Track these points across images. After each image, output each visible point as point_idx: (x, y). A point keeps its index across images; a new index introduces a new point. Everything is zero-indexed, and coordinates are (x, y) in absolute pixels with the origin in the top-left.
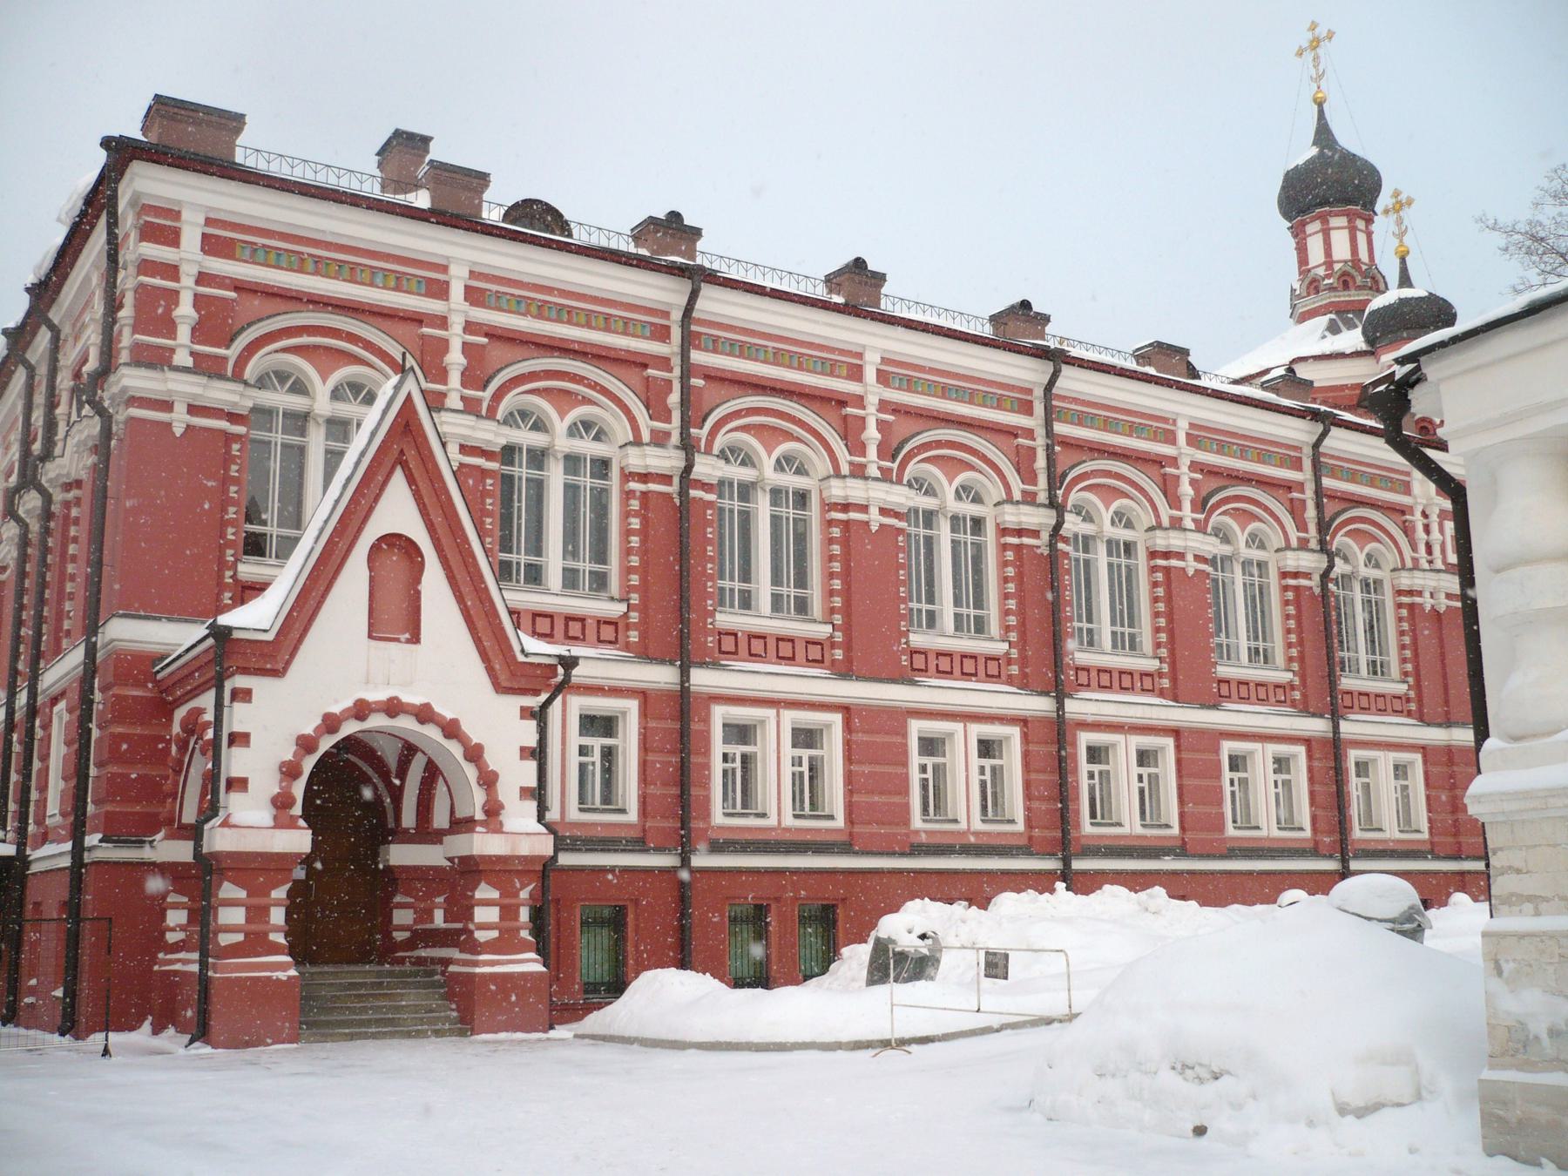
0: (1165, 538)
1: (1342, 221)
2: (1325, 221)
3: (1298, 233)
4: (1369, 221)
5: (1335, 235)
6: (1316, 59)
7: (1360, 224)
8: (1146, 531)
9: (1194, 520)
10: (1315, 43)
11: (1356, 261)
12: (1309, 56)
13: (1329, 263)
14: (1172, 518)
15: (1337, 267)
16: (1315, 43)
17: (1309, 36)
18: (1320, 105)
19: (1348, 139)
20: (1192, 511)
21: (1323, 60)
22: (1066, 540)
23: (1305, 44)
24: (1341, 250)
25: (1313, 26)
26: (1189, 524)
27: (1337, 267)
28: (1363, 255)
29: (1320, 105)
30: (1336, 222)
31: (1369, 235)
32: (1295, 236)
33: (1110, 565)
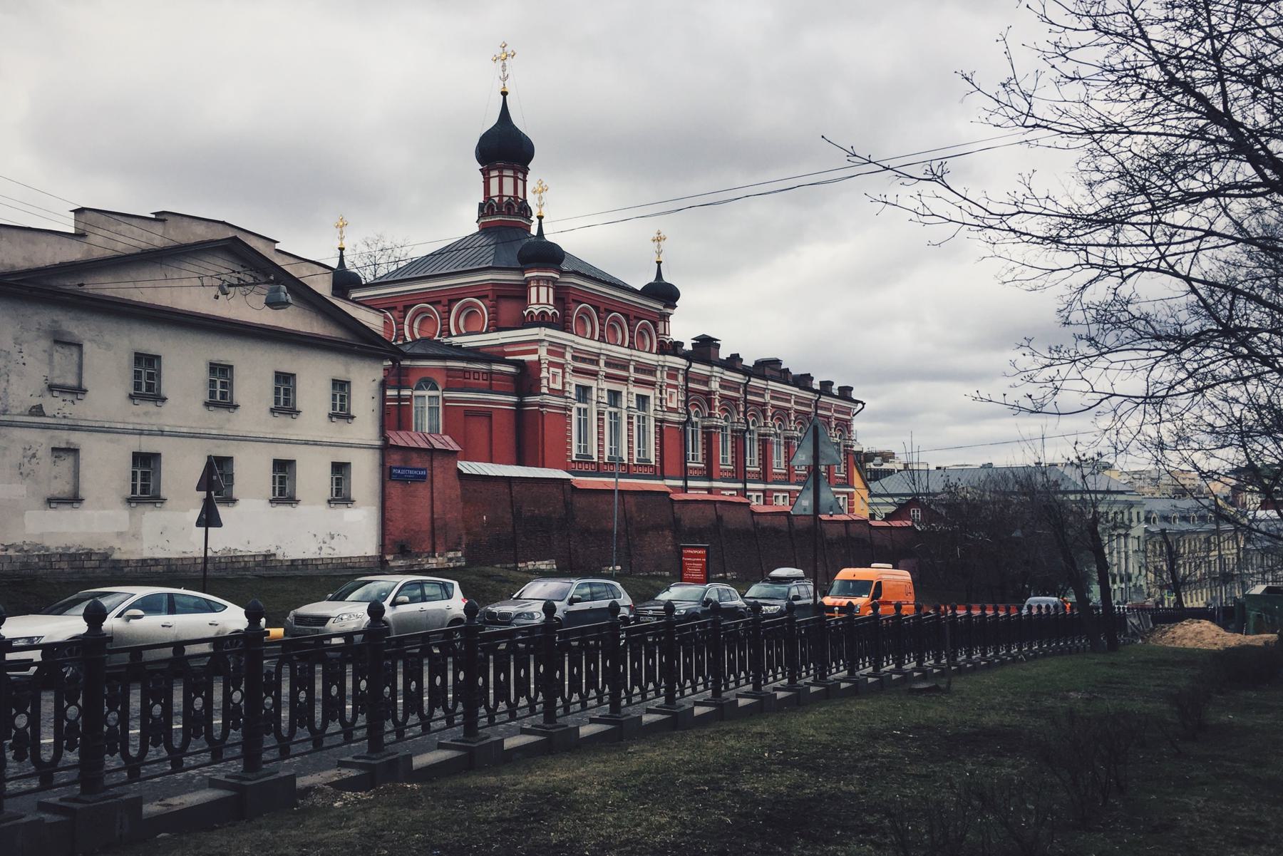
1: (510, 173)
2: (501, 172)
3: (486, 173)
4: (525, 174)
5: (505, 180)
6: (504, 66)
7: (520, 176)
11: (516, 197)
13: (501, 196)
15: (505, 199)
18: (504, 94)
19: (519, 120)
21: (507, 68)
24: (508, 190)
27: (505, 199)
28: (520, 195)
29: (504, 94)
30: (506, 173)
31: (525, 181)
32: (484, 175)
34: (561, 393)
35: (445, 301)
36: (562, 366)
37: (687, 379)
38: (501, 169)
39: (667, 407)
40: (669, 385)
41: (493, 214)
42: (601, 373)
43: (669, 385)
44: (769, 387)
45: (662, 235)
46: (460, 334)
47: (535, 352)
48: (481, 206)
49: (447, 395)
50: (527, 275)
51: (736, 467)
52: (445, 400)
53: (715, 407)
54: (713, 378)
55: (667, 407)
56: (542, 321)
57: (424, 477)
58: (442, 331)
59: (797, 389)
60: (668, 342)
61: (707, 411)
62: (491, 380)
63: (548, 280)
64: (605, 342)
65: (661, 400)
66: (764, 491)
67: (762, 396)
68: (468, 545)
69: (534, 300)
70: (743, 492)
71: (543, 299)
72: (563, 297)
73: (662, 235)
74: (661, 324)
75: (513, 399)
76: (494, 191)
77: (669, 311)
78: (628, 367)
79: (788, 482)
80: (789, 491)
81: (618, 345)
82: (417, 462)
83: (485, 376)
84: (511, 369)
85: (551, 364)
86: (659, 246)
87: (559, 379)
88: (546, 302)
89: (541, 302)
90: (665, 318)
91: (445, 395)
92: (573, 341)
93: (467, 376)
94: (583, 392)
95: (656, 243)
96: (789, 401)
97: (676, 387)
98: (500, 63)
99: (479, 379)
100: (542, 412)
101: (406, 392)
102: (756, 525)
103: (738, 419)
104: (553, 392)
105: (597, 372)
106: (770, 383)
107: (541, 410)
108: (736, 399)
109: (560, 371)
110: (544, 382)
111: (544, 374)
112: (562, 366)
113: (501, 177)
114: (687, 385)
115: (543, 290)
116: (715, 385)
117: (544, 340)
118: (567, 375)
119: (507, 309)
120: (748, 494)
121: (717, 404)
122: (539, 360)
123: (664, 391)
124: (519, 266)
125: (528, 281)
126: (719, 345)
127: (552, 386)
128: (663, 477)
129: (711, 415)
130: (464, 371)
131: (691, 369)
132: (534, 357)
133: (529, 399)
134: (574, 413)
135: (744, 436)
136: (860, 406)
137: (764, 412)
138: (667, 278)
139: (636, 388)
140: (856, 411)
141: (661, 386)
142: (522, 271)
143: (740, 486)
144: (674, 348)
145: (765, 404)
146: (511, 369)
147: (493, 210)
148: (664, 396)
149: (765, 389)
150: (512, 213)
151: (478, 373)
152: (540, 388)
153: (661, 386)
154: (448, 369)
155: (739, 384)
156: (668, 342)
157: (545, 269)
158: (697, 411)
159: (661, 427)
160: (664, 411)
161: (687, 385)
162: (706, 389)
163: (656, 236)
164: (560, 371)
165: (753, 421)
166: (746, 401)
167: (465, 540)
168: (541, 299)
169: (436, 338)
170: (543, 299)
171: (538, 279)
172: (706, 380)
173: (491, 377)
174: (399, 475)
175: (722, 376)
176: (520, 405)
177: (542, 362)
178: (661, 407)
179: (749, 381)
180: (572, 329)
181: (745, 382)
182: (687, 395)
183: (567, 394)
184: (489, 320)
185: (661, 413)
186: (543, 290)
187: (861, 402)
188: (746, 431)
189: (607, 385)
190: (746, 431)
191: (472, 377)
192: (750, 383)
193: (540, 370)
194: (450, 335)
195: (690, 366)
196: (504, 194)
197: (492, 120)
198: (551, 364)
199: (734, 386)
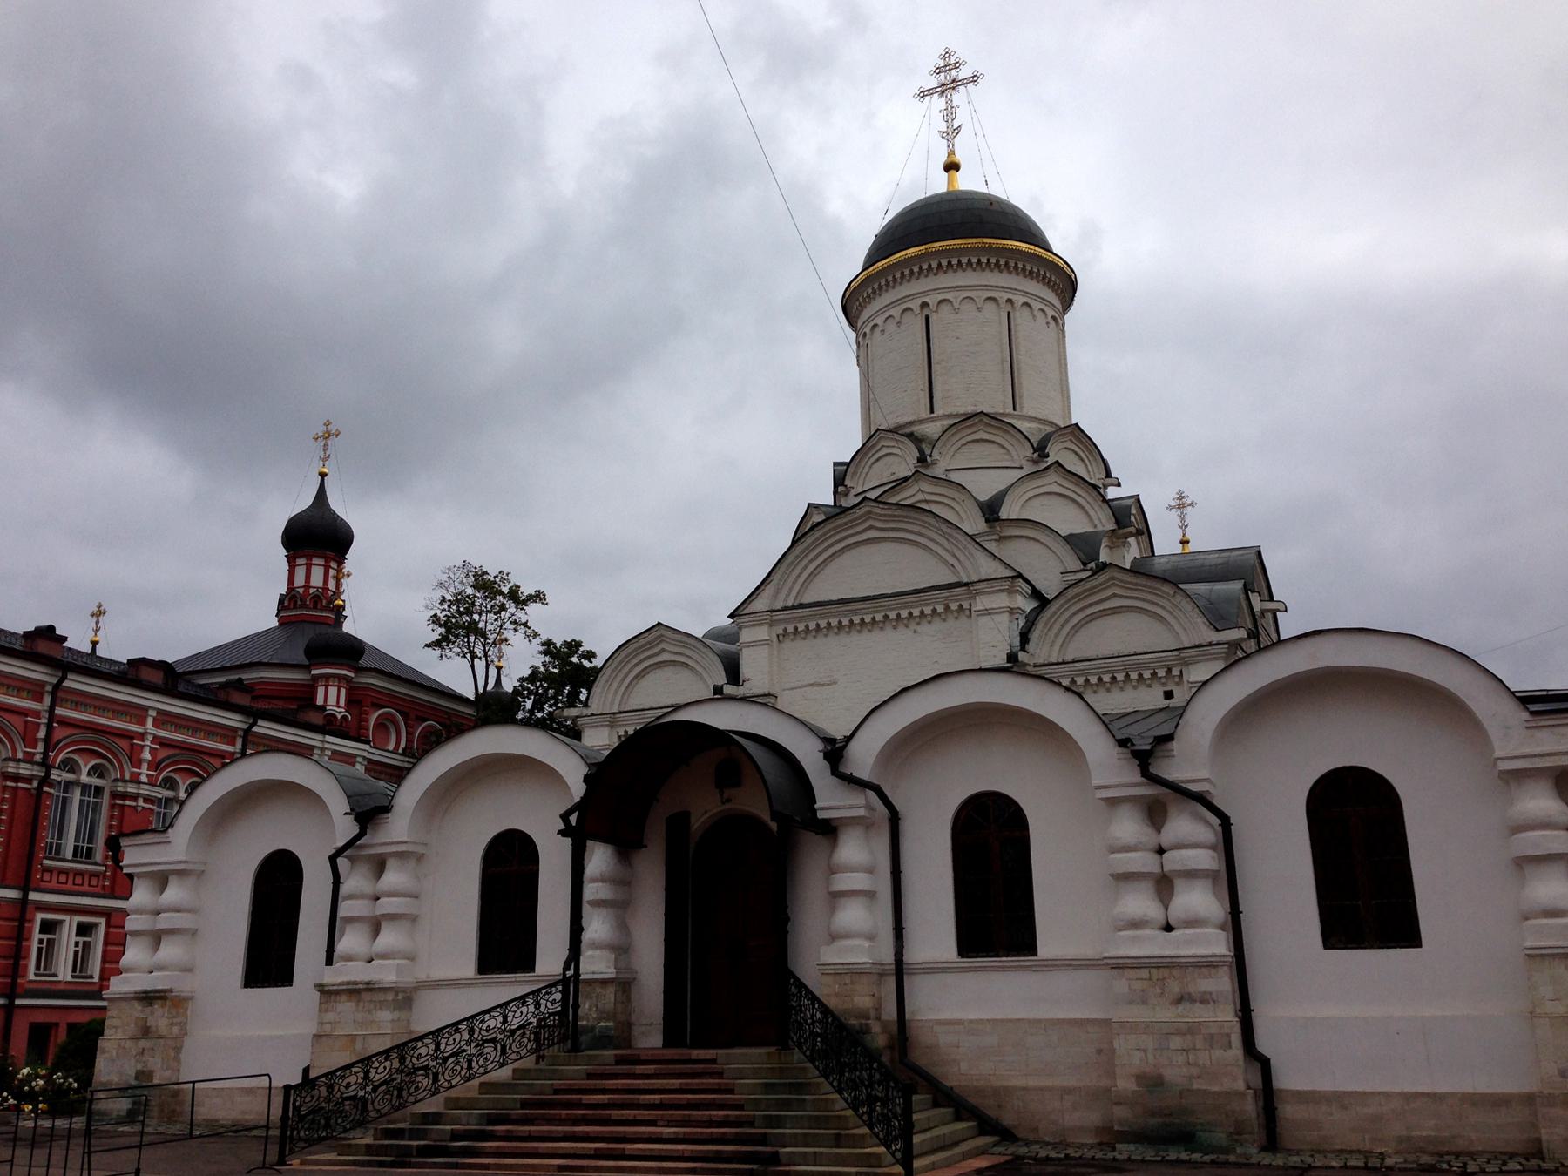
0: (124, 787)
1: (322, 562)
3: (291, 560)
7: (334, 565)
8: (112, 781)
9: (148, 775)
11: (325, 588)
13: (307, 587)
14: (132, 774)
15: (312, 591)
20: (148, 770)
22: (51, 785)
24: (317, 579)
26: (144, 778)
28: (332, 585)
30: (315, 561)
33: (82, 801)
38: (309, 557)
41: (295, 607)
48: (282, 599)
50: (313, 672)
72: (357, 699)
76: (300, 580)
113: (309, 566)
115: (333, 691)
124: (307, 663)
125: (316, 678)
142: (308, 668)
147: (296, 602)
150: (319, 607)
168: (332, 699)
171: (327, 677)
186: (333, 691)
196: (312, 584)
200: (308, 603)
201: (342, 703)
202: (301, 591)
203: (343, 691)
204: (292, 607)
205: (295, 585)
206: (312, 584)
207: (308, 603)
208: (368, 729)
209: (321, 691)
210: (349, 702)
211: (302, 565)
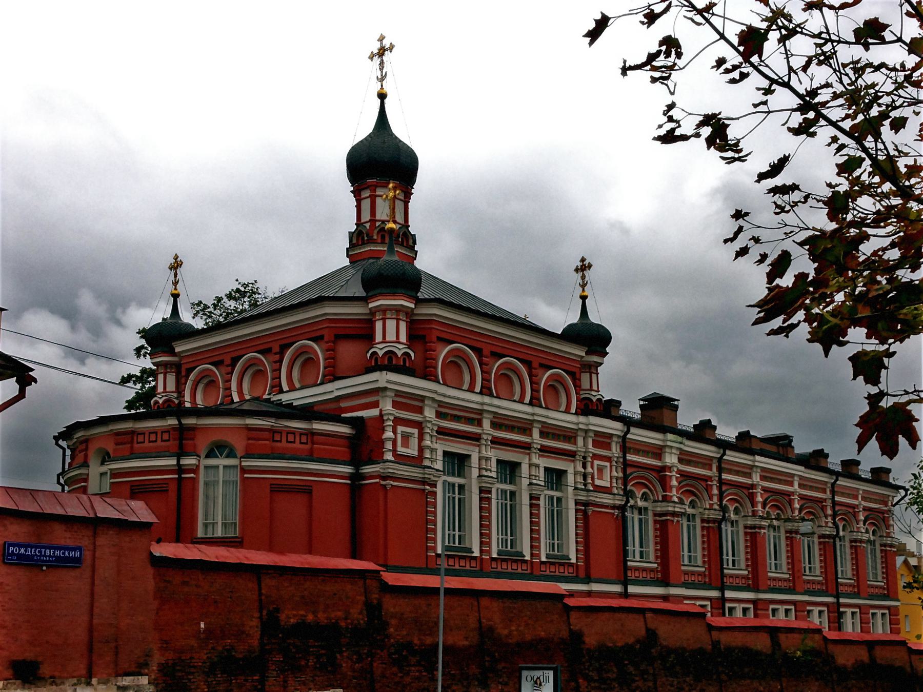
6: (382, 63)
10: (382, 52)
12: (377, 60)
13: (373, 221)
15: (378, 224)
16: (382, 52)
17: (378, 45)
18: (382, 96)
19: (400, 129)
23: (376, 51)
25: (381, 39)
34: (417, 461)
35: (276, 349)
36: (419, 425)
37: (625, 449)
38: (373, 188)
39: (593, 485)
40: (596, 457)
42: (485, 437)
43: (596, 457)
44: (757, 464)
45: (586, 263)
46: (292, 389)
47: (375, 405)
49: (247, 463)
50: (371, 305)
51: (709, 569)
52: (244, 470)
53: (671, 487)
54: (668, 450)
55: (593, 485)
56: (390, 363)
57: (78, 560)
58: (272, 387)
59: (802, 468)
60: (594, 399)
61: (661, 494)
62: (313, 443)
63: (398, 310)
64: (490, 395)
65: (585, 476)
66: (755, 602)
67: (749, 475)
68: (162, 668)
69: (379, 337)
70: (720, 604)
71: (391, 336)
73: (586, 263)
74: (585, 378)
75: (347, 469)
76: (366, 216)
77: (596, 359)
78: (531, 430)
79: (791, 591)
80: (794, 603)
81: (515, 401)
82: (61, 536)
83: (304, 439)
84: (344, 430)
85: (398, 421)
86: (583, 277)
87: (414, 442)
88: (395, 339)
89: (387, 339)
90: (593, 368)
91: (243, 464)
92: (435, 392)
93: (277, 437)
94: (457, 463)
95: (580, 274)
96: (791, 484)
97: (609, 459)
98: (377, 60)
99: (294, 442)
100: (385, 486)
101: (188, 461)
102: (716, 644)
103: (711, 505)
104: (401, 459)
105: (480, 435)
106: (758, 458)
107: (383, 483)
108: (706, 479)
109: (416, 431)
110: (389, 445)
111: (389, 434)
112: (419, 425)
113: (373, 198)
114: (624, 457)
115: (391, 324)
116: (671, 459)
117: (385, 389)
118: (427, 437)
119: (348, 351)
120: (728, 605)
121: (674, 482)
122: (381, 415)
123: (589, 465)
124: (364, 294)
125: (373, 312)
126: (677, 407)
127: (401, 449)
128: (588, 580)
129: (666, 499)
130: (272, 431)
131: (629, 436)
132: (374, 412)
133: (368, 469)
134: (439, 490)
135: (720, 529)
136: (903, 492)
137: (752, 497)
138: (594, 318)
139: (545, 459)
140: (896, 500)
141: (584, 458)
142: (364, 300)
143: (715, 594)
144: (609, 409)
145: (753, 486)
146: (344, 430)
148: (589, 470)
149: (751, 467)
151: (294, 433)
152: (383, 453)
153: (584, 458)
154: (249, 428)
155: (711, 458)
156: (594, 399)
157: (394, 295)
158: (644, 494)
159: (585, 513)
160: (589, 491)
161: (624, 457)
162: (660, 464)
163: (579, 264)
164: (416, 431)
165: (736, 509)
166: (721, 482)
167: (157, 659)
169: (265, 397)
170: (391, 336)
171: (384, 310)
172: (658, 452)
173: (312, 440)
174: (20, 556)
175: (682, 446)
176: (356, 477)
177: (385, 418)
178: (585, 485)
179: (724, 454)
180: (436, 376)
181: (719, 456)
182: (624, 471)
183: (427, 463)
184: (325, 368)
185: (584, 493)
186: (391, 324)
187: (903, 488)
188: (722, 520)
189: (494, 454)
190: (722, 520)
191: (284, 440)
192: (725, 457)
193: (383, 430)
194: (281, 391)
195: (628, 432)
196: (378, 217)
197: (366, 127)
198: (398, 421)
199: (705, 462)
200: (375, 237)
201: (403, 338)
202: (368, 225)
203: (403, 326)
204: (360, 243)
205: (362, 221)
206: (378, 217)
207: (375, 237)
208: (436, 368)
209: (379, 325)
210: (411, 337)
211: (367, 197)
